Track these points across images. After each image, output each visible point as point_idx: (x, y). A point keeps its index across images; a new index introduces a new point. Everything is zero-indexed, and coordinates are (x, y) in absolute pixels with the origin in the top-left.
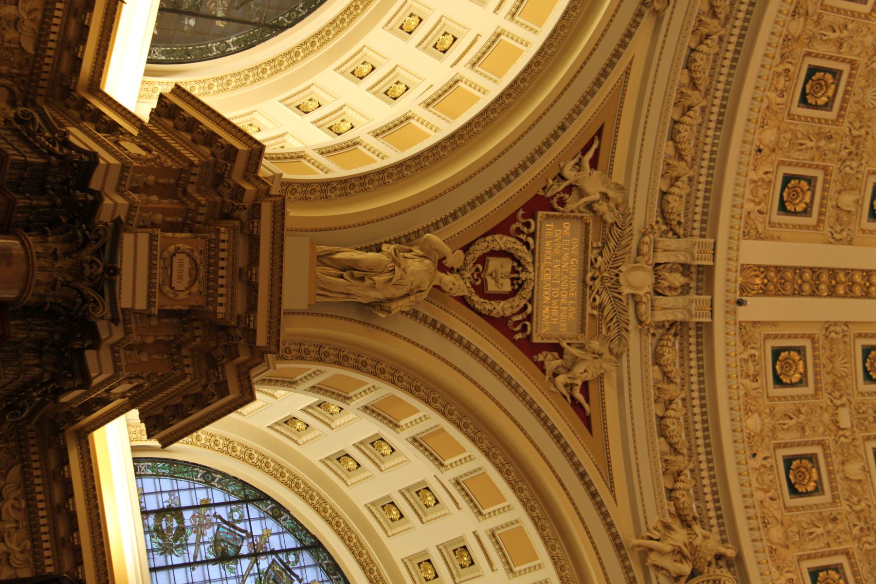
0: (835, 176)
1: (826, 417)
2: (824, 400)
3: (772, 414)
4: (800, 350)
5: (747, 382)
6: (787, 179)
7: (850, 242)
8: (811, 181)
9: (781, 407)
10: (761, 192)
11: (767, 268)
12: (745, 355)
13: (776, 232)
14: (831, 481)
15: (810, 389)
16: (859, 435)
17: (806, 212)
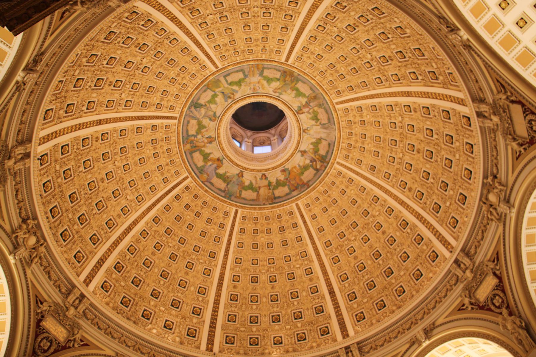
0: (188, 323)
1: (242, 333)
2: (238, 333)
3: (240, 347)
4: (227, 337)
5: (232, 352)
6: (188, 335)
7: (204, 321)
8: (189, 329)
9: (239, 344)
10: (190, 342)
11: (207, 343)
12: (226, 351)
13: (199, 340)
14: (256, 335)
15: (235, 336)
16: (247, 326)
17: (196, 330)
